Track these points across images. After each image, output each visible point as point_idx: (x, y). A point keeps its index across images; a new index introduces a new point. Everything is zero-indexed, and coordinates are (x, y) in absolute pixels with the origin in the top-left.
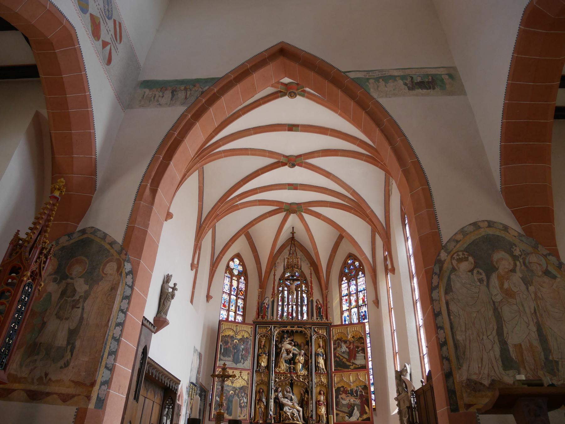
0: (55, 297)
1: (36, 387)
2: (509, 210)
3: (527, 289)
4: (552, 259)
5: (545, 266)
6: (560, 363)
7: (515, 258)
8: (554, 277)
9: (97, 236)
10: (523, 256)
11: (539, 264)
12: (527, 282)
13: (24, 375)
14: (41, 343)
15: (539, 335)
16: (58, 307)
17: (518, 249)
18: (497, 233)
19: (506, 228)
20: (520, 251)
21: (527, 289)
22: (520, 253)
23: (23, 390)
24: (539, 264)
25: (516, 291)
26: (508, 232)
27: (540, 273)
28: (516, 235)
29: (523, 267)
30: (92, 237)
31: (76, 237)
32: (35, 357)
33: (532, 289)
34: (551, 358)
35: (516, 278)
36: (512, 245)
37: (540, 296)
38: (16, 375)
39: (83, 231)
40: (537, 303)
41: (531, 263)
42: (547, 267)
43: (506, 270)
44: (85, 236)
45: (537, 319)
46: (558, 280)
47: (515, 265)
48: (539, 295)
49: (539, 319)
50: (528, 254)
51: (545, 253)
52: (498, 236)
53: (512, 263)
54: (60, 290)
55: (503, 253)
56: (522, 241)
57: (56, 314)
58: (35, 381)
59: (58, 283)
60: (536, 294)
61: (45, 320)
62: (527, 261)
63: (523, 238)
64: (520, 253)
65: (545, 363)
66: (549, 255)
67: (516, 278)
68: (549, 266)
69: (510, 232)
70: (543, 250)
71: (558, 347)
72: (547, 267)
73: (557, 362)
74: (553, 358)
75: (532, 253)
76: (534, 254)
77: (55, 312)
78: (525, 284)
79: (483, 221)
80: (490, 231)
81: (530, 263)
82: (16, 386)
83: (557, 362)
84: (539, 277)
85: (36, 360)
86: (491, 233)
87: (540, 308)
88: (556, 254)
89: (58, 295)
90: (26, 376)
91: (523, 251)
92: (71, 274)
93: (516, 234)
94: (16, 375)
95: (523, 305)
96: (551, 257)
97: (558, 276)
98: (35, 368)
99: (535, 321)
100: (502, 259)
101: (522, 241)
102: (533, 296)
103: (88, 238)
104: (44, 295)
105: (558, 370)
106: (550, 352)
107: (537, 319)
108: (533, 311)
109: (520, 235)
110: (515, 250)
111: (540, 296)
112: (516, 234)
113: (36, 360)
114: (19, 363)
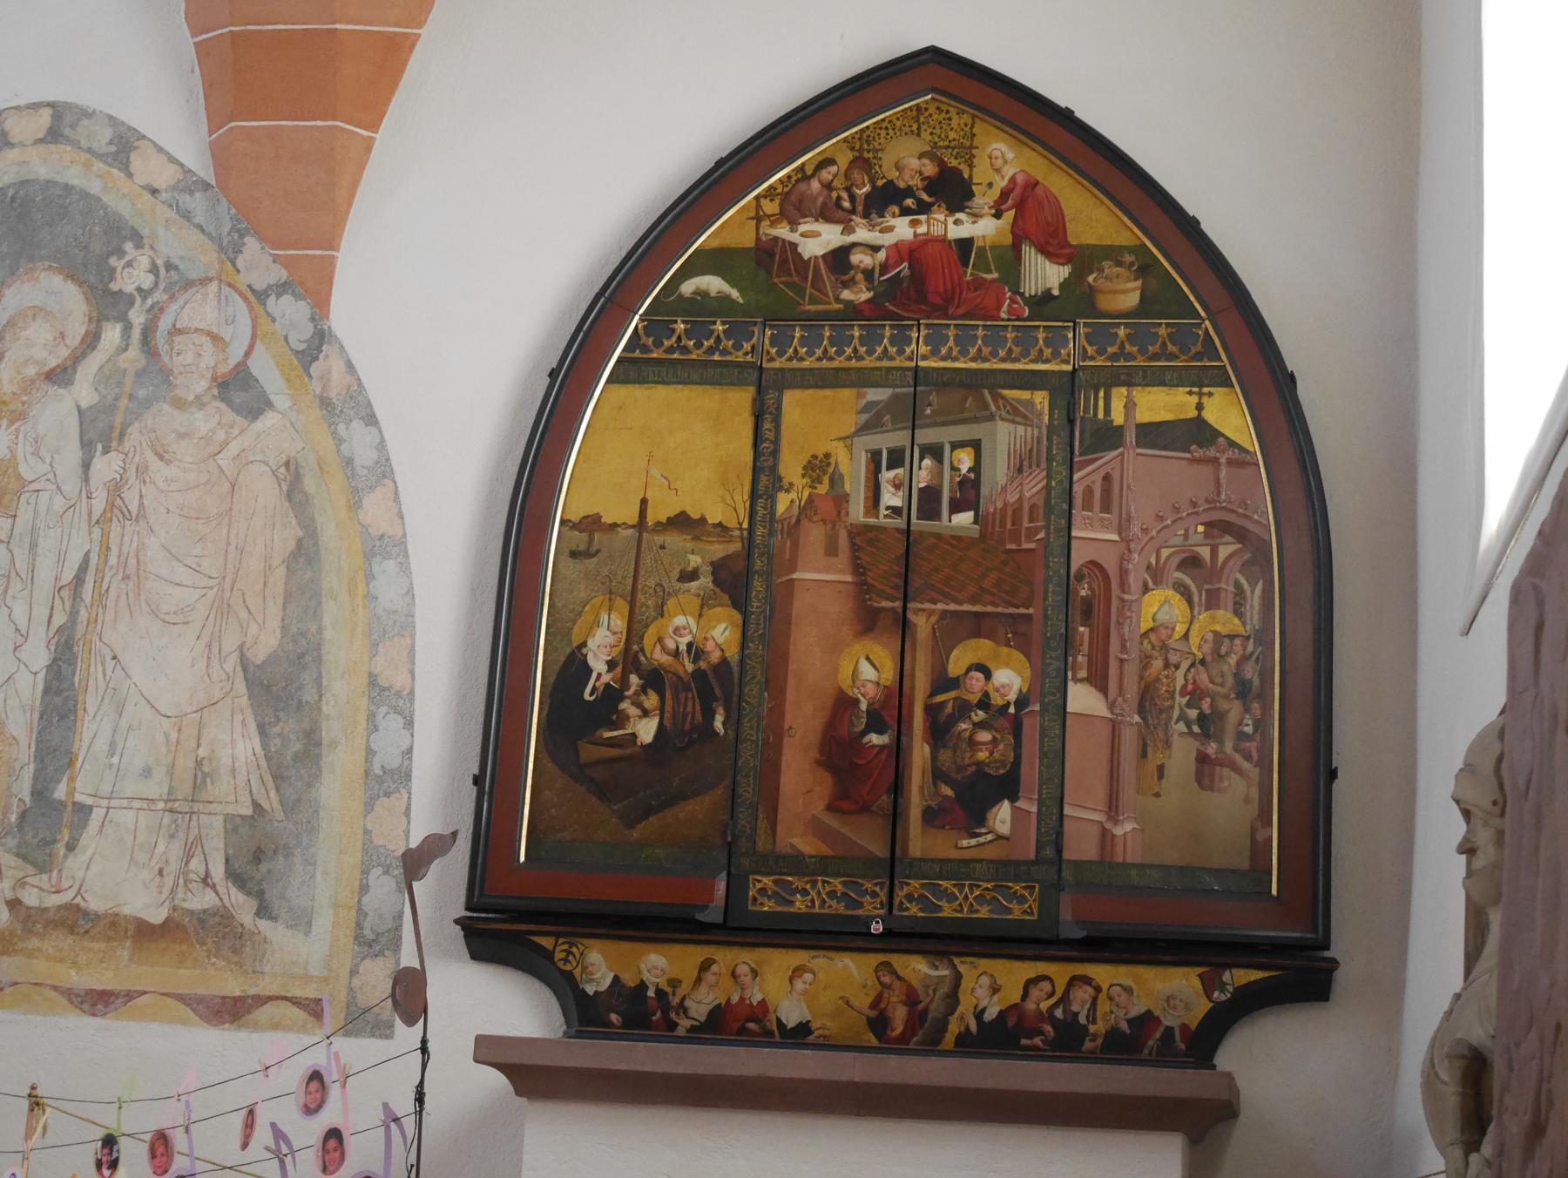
2: (186, 43)
3: (86, 465)
4: (291, 312)
5: (235, 355)
6: (97, 815)
7: (108, 304)
8: (257, 405)
10: (159, 296)
11: (216, 338)
12: (98, 432)
15: (46, 691)
17: (144, 262)
18: (74, 176)
19: (124, 145)
20: (154, 269)
21: (86, 465)
22: (147, 281)
24: (216, 338)
25: (28, 476)
26: (126, 168)
27: (201, 385)
28: (160, 183)
29: (134, 352)
33: (106, 466)
34: (60, 792)
35: (58, 414)
36: (120, 234)
37: (134, 507)
40: (105, 536)
41: (180, 332)
42: (248, 354)
43: (31, 371)
45: (74, 614)
46: (269, 420)
47: (91, 341)
48: (131, 498)
49: (83, 614)
50: (188, 284)
51: (259, 286)
52: (68, 189)
53: (77, 330)
55: (57, 281)
56: (186, 215)
60: (116, 489)
62: (165, 323)
63: (197, 203)
64: (147, 281)
65: (23, 815)
66: (282, 288)
67: (58, 414)
68: (260, 348)
69: (136, 163)
70: (259, 264)
71: (113, 745)
72: (248, 354)
73: (83, 811)
74: (71, 791)
75: (204, 281)
76: (213, 287)
78: (87, 446)
79: (35, 106)
80: (45, 165)
81: (175, 331)
83: (83, 811)
84: (179, 404)
86: (42, 172)
87: (113, 560)
88: (313, 285)
91: (169, 266)
93: (164, 177)
95: (33, 546)
96: (286, 299)
97: (281, 401)
99: (60, 619)
100: (38, 312)
101: (186, 215)
102: (99, 505)
105: (71, 848)
106: (71, 763)
107: (74, 614)
108: (68, 575)
109: (189, 183)
110: (129, 264)
111: (134, 507)
112: (164, 177)
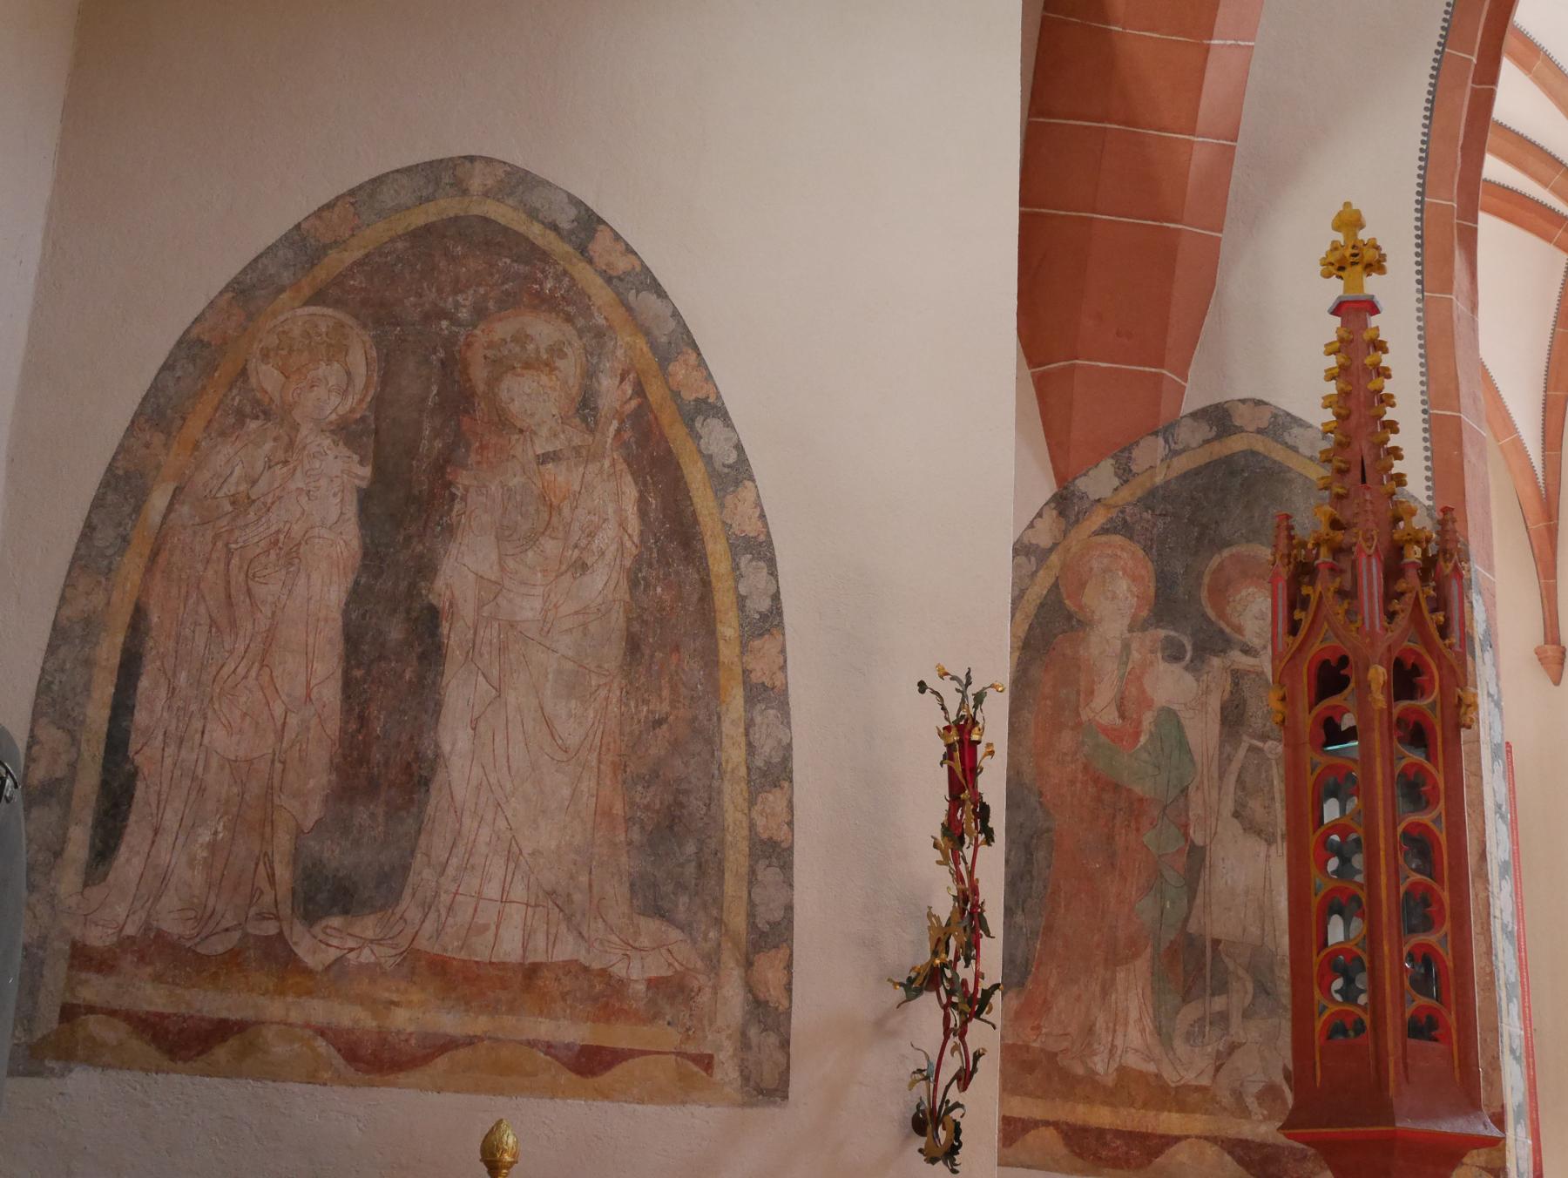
0: (1203, 732)
1: (1263, 1129)
9: (1295, 449)
13: (1190, 1077)
14: (1216, 942)
16: (1232, 779)
23: (1213, 1140)
30: (1278, 454)
31: (1197, 448)
32: (1219, 1003)
38: (1158, 1076)
39: (1219, 418)
44: (1236, 444)
54: (1215, 703)
57: (1236, 815)
58: (1251, 1101)
59: (1193, 668)
61: (1198, 837)
77: (1228, 806)
82: (1170, 1122)
85: (1223, 1018)
89: (1215, 727)
90: (1205, 1081)
92: (1239, 629)
94: (1158, 1076)
98: (1233, 1048)
103: (1254, 453)
104: (1148, 718)
113: (1223, 1018)
114: (1148, 1024)
